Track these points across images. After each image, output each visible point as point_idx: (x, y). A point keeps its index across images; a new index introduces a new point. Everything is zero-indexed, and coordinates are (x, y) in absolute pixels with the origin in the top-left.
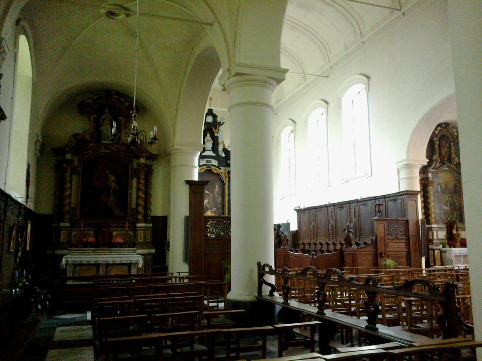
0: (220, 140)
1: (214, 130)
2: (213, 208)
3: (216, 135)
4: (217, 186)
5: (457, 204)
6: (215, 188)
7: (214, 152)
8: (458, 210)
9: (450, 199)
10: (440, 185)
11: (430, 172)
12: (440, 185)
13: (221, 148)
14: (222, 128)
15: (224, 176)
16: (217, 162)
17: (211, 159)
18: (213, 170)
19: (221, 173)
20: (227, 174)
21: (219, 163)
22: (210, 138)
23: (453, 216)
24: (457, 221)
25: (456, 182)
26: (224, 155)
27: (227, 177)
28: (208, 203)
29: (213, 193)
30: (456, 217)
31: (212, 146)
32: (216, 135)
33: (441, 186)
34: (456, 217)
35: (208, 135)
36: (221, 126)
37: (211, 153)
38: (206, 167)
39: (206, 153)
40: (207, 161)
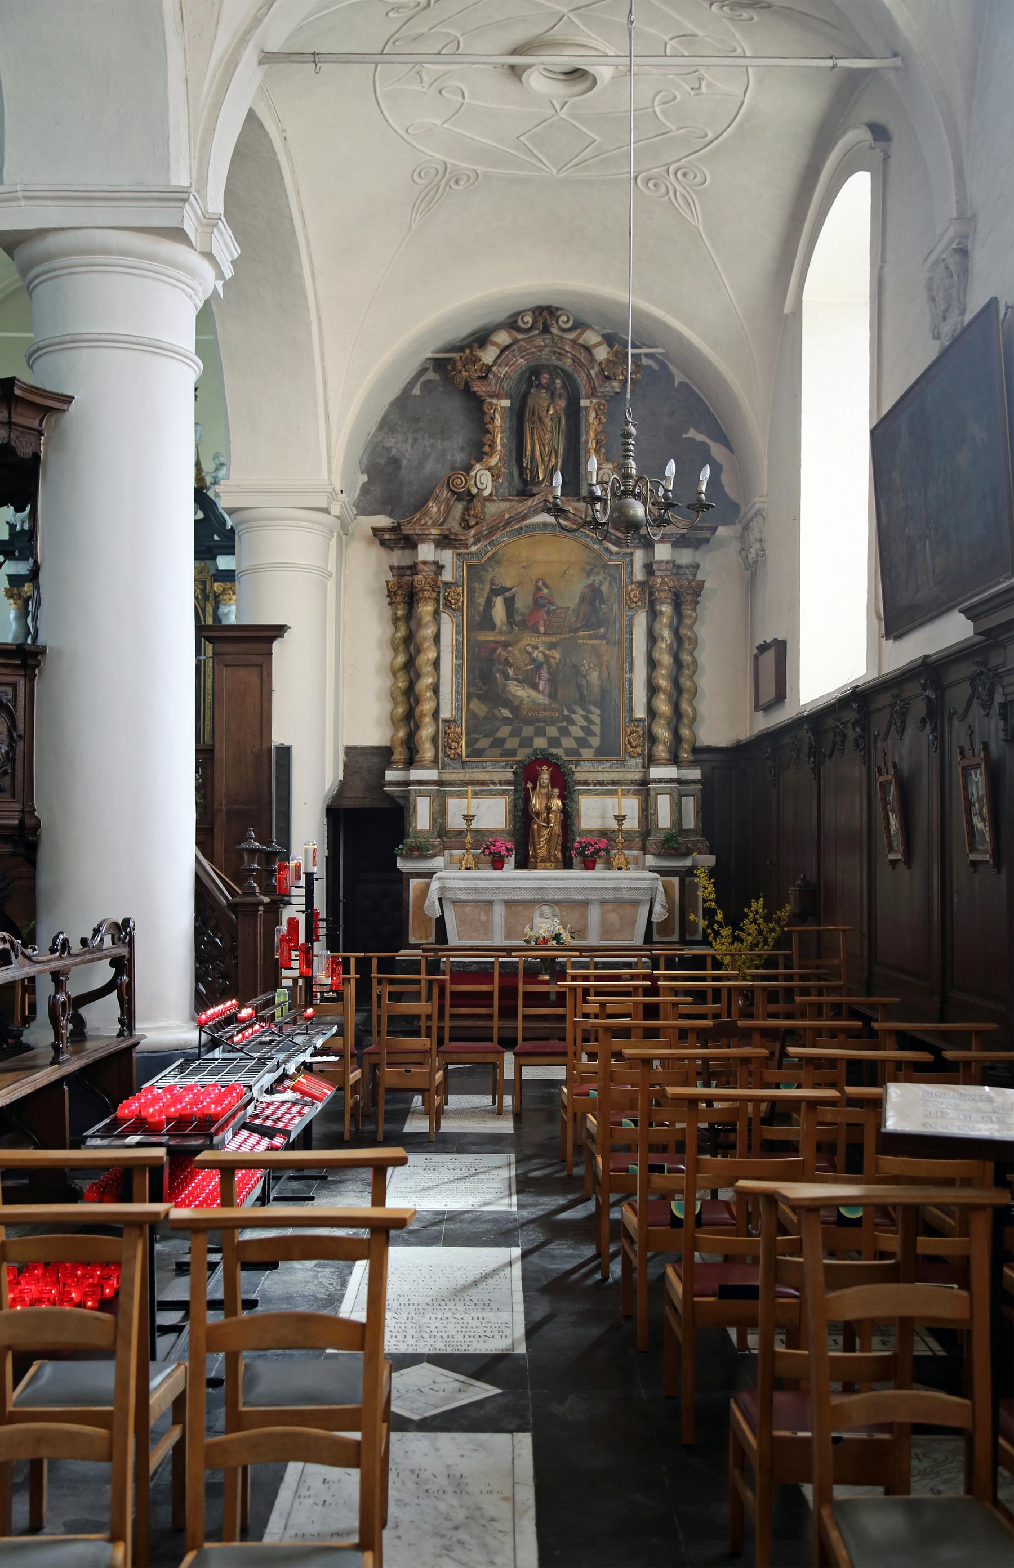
5: (595, 675)
8: (595, 705)
9: (556, 655)
10: (508, 594)
11: (423, 538)
12: (508, 594)
23: (565, 732)
24: (587, 753)
25: (596, 579)
30: (581, 734)
33: (510, 604)
34: (581, 734)
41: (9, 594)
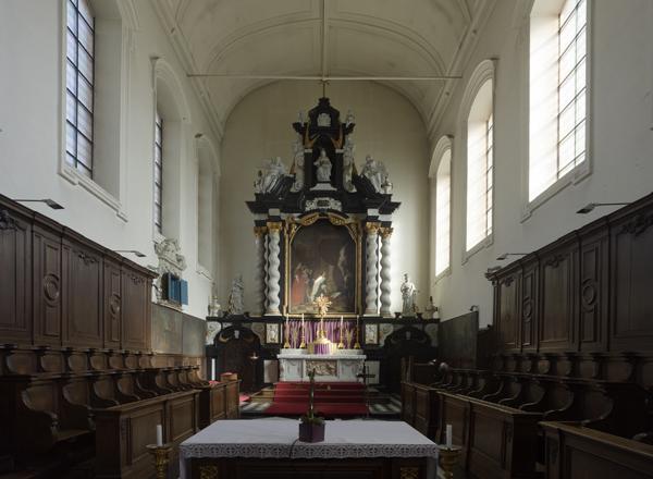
0: (347, 162)
1: (333, 141)
2: (334, 292)
3: (338, 151)
4: (342, 252)
6: (339, 255)
7: (333, 185)
13: (348, 178)
14: (350, 138)
15: (354, 229)
16: (340, 204)
17: (327, 199)
18: (332, 220)
19: (349, 225)
20: (360, 226)
21: (343, 206)
22: (327, 159)
26: (355, 190)
27: (361, 231)
28: (325, 283)
29: (335, 264)
31: (329, 173)
32: (338, 151)
35: (324, 153)
36: (350, 135)
37: (328, 187)
38: (317, 214)
39: (319, 187)
40: (319, 203)
41: (256, 232)
